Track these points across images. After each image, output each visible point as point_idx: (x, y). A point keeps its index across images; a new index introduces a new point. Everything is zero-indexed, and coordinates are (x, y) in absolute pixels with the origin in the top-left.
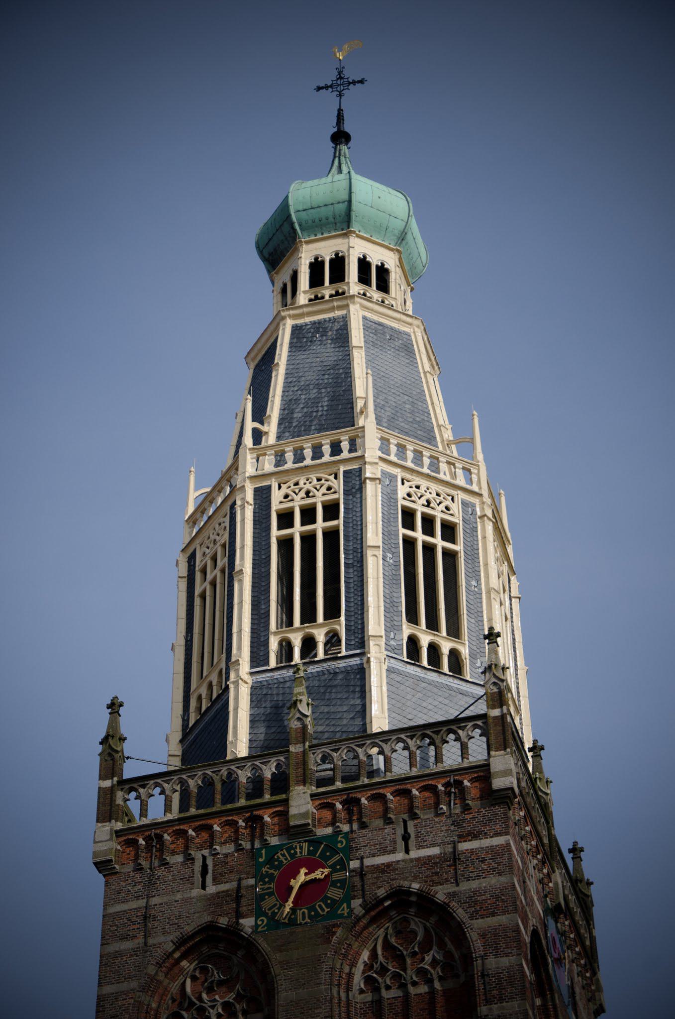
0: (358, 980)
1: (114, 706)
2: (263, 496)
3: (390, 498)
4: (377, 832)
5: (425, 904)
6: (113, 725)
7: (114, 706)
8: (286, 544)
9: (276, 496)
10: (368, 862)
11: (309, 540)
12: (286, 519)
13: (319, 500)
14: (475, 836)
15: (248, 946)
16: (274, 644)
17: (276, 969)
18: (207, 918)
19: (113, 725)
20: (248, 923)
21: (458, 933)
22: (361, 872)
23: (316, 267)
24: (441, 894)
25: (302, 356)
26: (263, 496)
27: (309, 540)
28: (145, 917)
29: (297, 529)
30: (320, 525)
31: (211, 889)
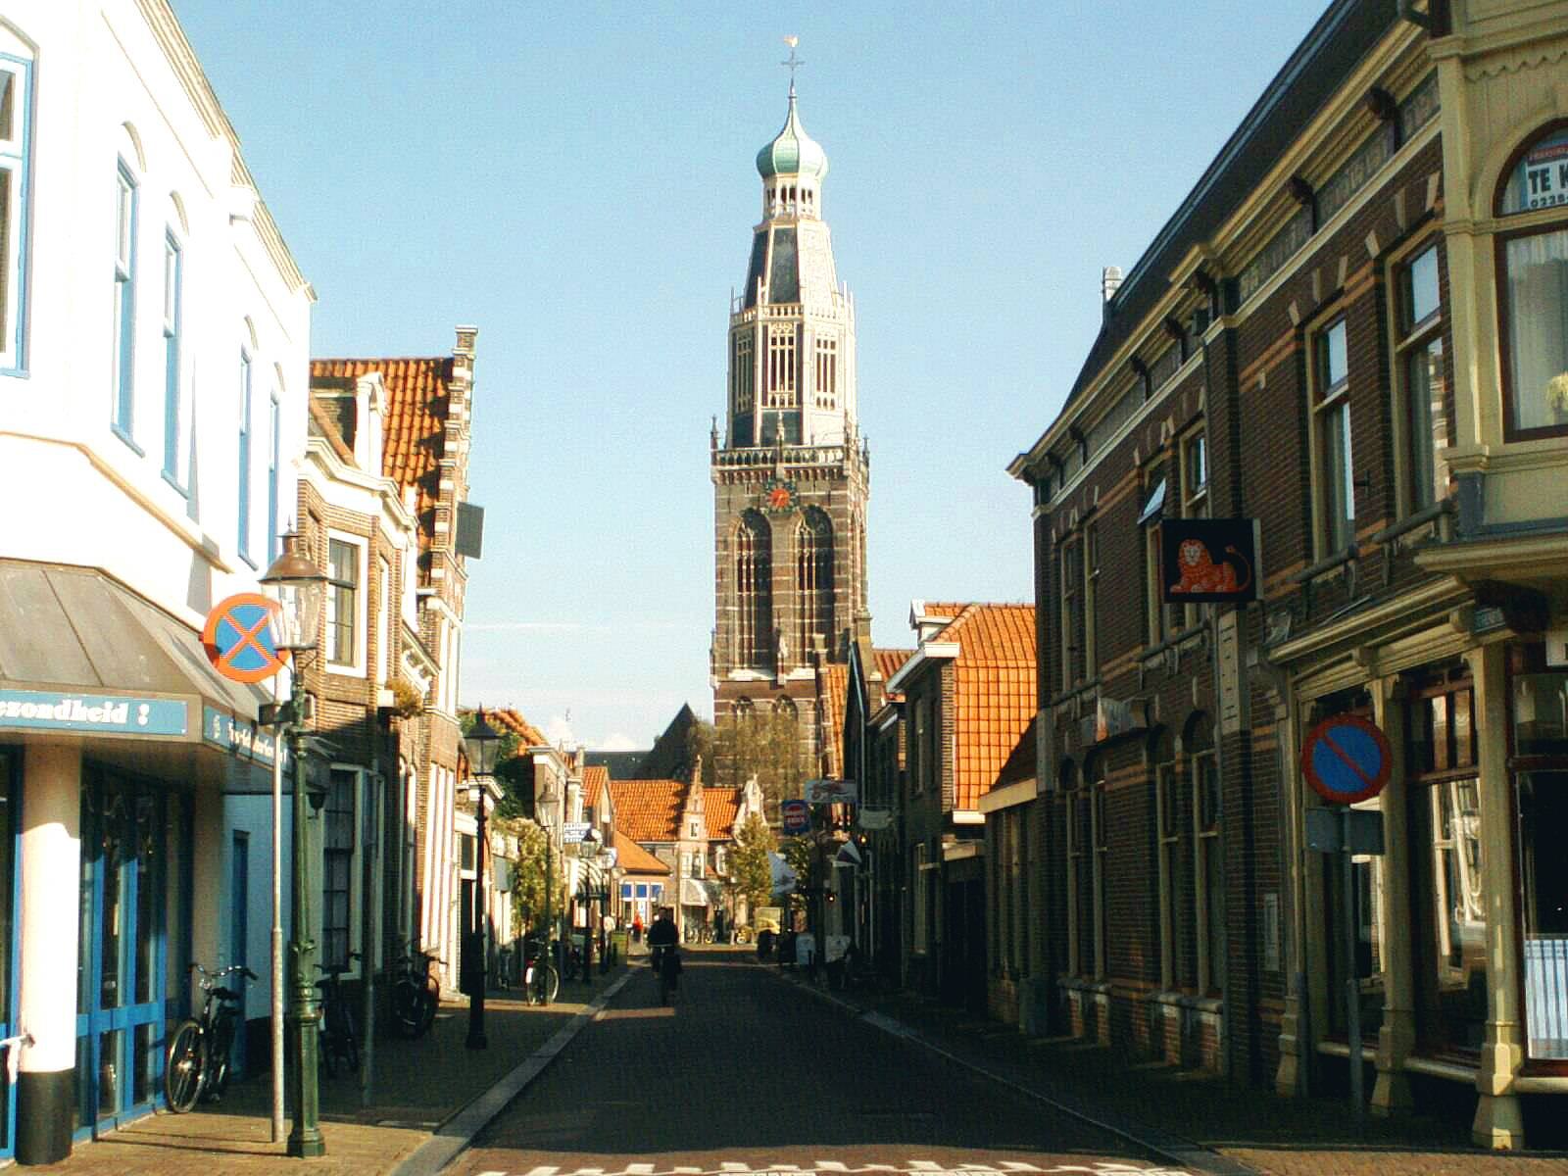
0: (797, 532)
1: (714, 419)
2: (765, 328)
3: (813, 335)
4: (803, 484)
5: (819, 510)
6: (714, 426)
7: (714, 419)
8: (774, 352)
9: (771, 329)
10: (802, 494)
11: (782, 352)
12: (774, 342)
13: (787, 336)
14: (836, 489)
15: (763, 517)
16: (770, 398)
17: (772, 526)
18: (748, 506)
19: (714, 426)
20: (763, 509)
21: (829, 522)
22: (799, 497)
23: (784, 191)
24: (825, 508)
25: (779, 248)
26: (765, 328)
27: (782, 352)
28: (729, 503)
29: (778, 347)
30: (787, 347)
31: (751, 495)
